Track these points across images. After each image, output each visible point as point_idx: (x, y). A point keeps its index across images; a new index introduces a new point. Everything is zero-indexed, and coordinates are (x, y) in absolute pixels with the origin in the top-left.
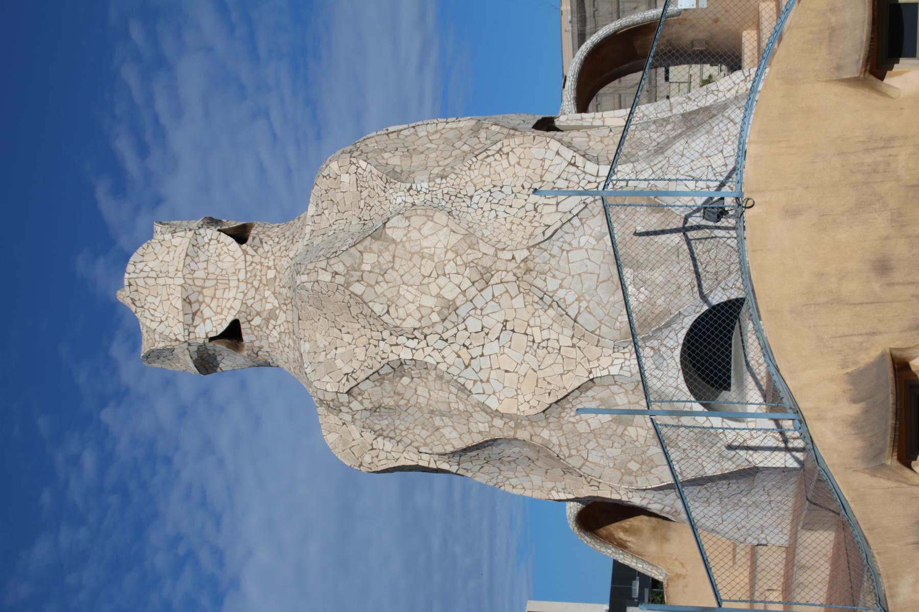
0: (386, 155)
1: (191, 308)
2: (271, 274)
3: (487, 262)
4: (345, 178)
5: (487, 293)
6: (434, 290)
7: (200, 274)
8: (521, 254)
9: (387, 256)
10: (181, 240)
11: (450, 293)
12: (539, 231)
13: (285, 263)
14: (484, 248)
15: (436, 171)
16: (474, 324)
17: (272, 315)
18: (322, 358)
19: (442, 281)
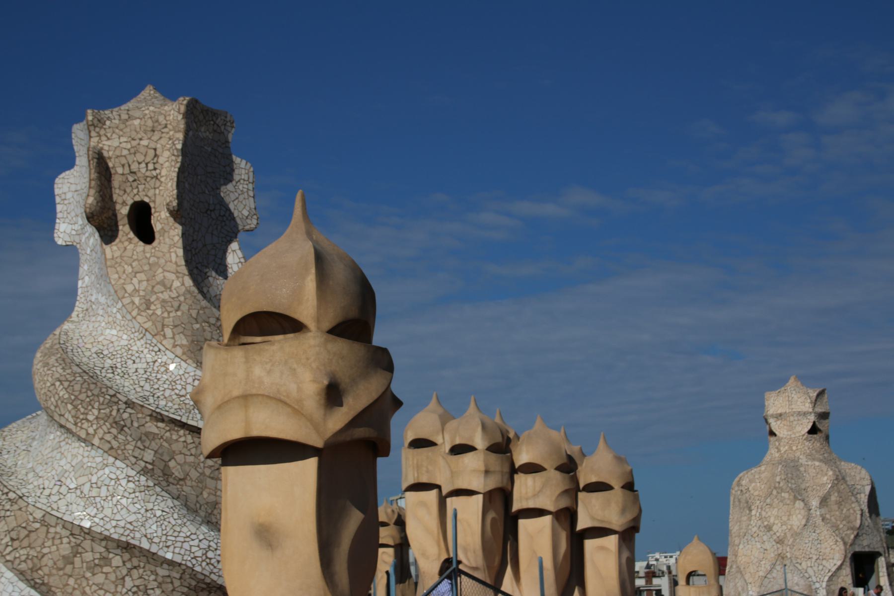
0: (836, 494)
1: (779, 416)
2: (794, 448)
3: (786, 542)
4: (825, 478)
5: (774, 543)
6: (776, 522)
7: (792, 418)
8: (788, 555)
9: (788, 502)
10: (807, 407)
11: (775, 528)
12: (799, 561)
13: (798, 454)
14: (791, 540)
15: (828, 516)
16: (765, 538)
17: (779, 451)
18: (757, 476)
19: (779, 525)
